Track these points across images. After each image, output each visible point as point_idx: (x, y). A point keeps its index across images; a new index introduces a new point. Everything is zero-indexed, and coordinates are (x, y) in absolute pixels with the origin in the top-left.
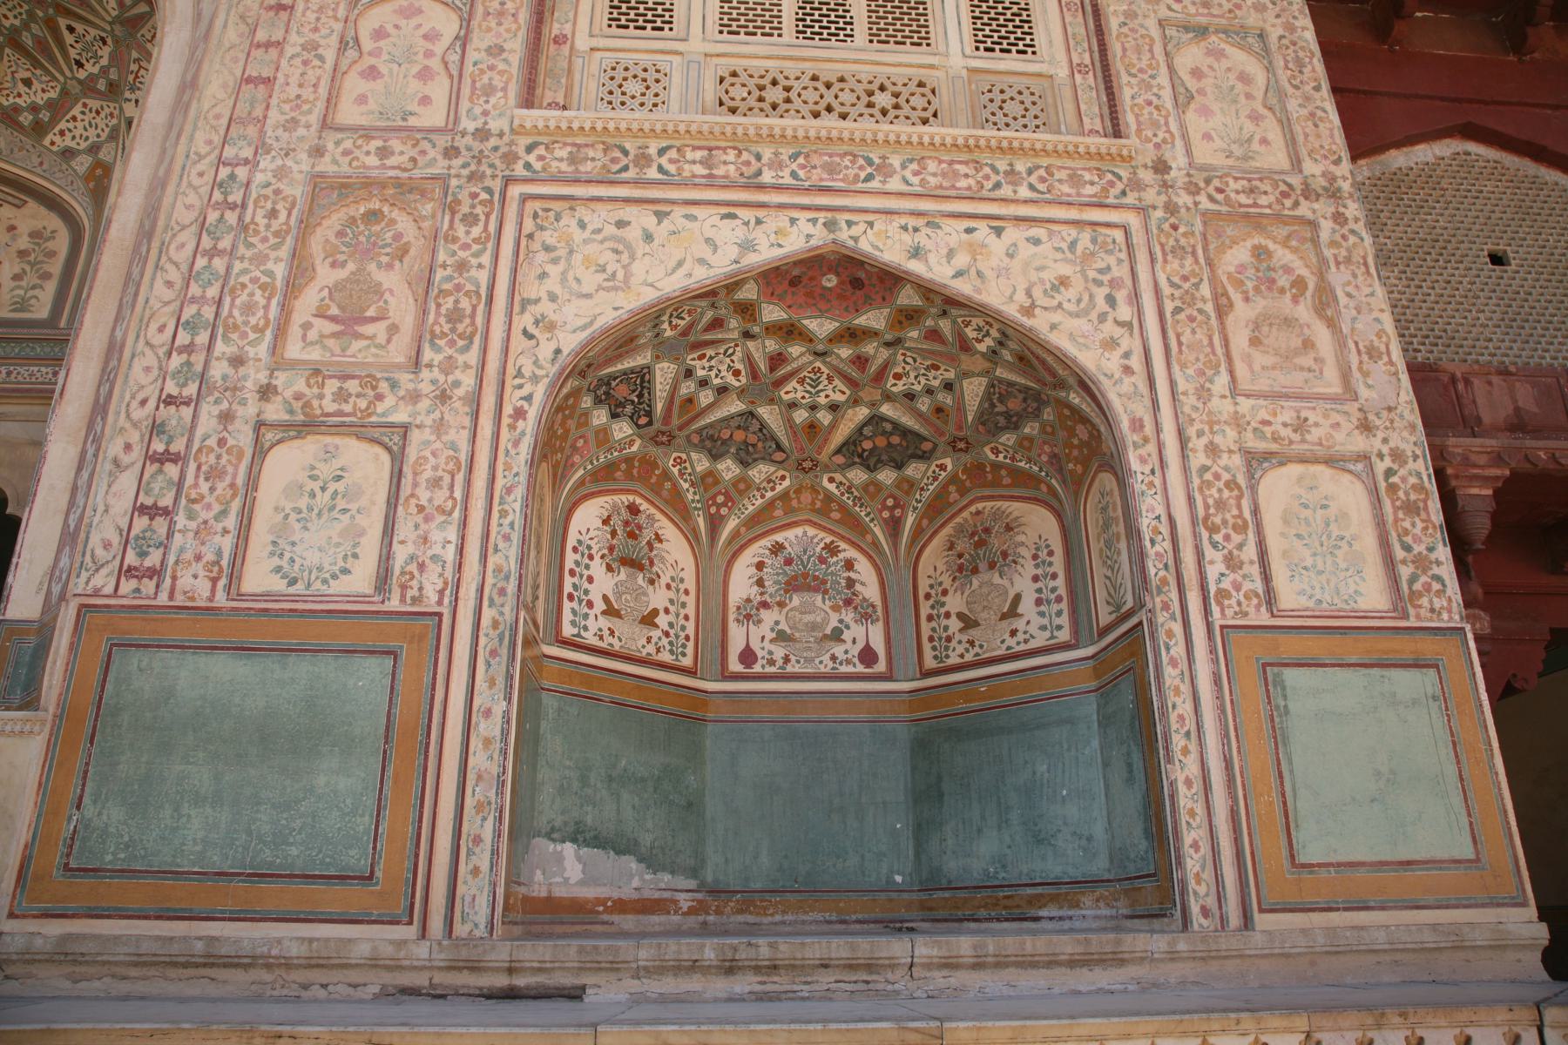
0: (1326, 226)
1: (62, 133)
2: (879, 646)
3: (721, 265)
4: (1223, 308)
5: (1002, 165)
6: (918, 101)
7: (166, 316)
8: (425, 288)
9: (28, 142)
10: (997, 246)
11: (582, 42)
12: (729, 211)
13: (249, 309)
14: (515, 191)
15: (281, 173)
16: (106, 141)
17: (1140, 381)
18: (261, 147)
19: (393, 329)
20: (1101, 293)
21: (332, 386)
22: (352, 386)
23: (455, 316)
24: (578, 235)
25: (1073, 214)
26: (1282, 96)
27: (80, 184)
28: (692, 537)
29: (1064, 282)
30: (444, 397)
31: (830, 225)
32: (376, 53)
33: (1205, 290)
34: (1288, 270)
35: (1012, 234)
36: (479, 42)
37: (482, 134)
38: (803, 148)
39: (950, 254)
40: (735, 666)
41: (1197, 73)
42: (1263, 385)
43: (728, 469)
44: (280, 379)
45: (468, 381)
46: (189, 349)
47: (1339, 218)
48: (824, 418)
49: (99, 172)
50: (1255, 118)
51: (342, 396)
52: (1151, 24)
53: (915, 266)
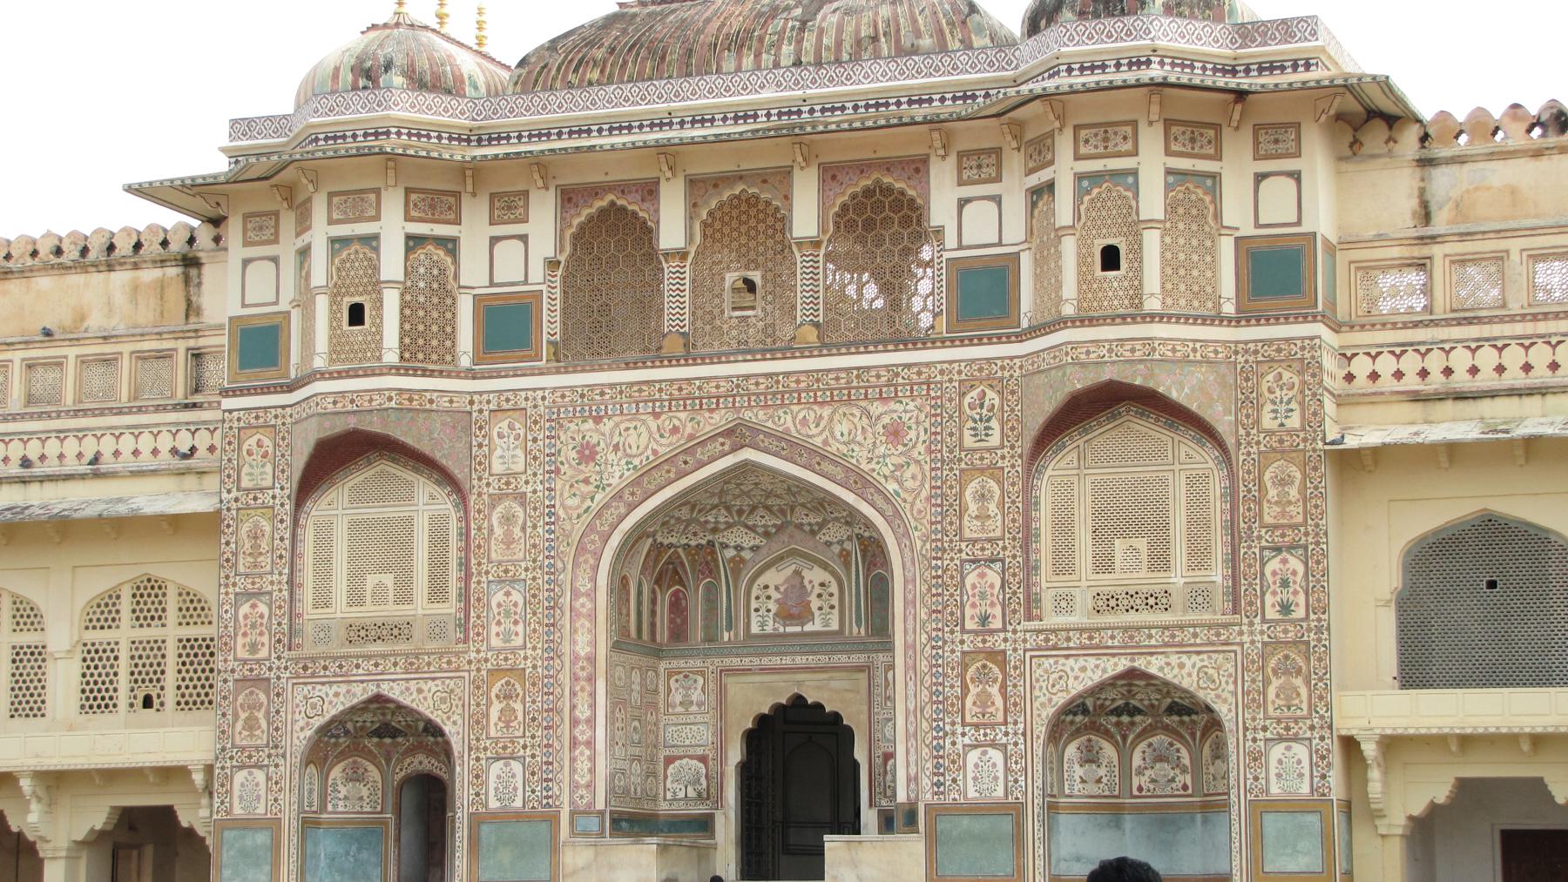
2: (1189, 782)
3: (1097, 677)
4: (1266, 682)
11: (1044, 585)
14: (1028, 654)
17: (1233, 714)
18: (945, 642)
23: (1015, 704)
28: (1116, 745)
30: (1015, 734)
31: (1133, 660)
40: (1135, 793)
41: (1274, 573)
43: (1125, 719)
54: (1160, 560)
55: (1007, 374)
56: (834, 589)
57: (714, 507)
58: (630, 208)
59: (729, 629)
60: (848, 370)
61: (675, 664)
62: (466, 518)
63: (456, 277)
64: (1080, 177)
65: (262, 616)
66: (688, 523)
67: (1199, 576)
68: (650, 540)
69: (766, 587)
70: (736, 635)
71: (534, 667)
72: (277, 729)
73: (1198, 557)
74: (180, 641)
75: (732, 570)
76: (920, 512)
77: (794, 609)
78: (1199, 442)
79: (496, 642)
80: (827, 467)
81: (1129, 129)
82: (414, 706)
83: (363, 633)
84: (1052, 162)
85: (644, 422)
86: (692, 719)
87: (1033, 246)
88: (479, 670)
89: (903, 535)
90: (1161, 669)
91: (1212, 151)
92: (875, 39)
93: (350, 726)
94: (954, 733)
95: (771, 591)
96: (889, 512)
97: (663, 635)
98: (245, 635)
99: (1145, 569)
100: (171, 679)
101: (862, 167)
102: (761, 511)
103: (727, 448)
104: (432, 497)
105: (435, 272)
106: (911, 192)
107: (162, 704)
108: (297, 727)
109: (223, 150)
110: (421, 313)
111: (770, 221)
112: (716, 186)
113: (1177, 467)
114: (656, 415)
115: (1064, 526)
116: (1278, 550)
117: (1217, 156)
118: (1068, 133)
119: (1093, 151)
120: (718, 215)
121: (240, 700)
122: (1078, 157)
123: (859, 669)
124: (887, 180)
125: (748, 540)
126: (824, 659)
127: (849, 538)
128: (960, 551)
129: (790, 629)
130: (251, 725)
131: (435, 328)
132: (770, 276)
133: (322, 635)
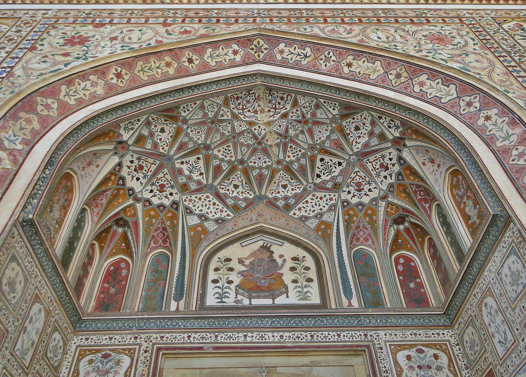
1: (300, 209)
16: (327, 211)
27: (312, 233)
49: (323, 226)
56: (310, 262)
59: (178, 298)
61: (94, 339)
66: (165, 161)
68: (116, 160)
70: (188, 304)
75: (192, 239)
77: (263, 277)
80: (361, 66)
85: (151, 28)
95: (234, 264)
102: (238, 177)
103: (238, 58)
114: (165, 24)
125: (214, 210)
127: (332, 208)
129: (256, 302)
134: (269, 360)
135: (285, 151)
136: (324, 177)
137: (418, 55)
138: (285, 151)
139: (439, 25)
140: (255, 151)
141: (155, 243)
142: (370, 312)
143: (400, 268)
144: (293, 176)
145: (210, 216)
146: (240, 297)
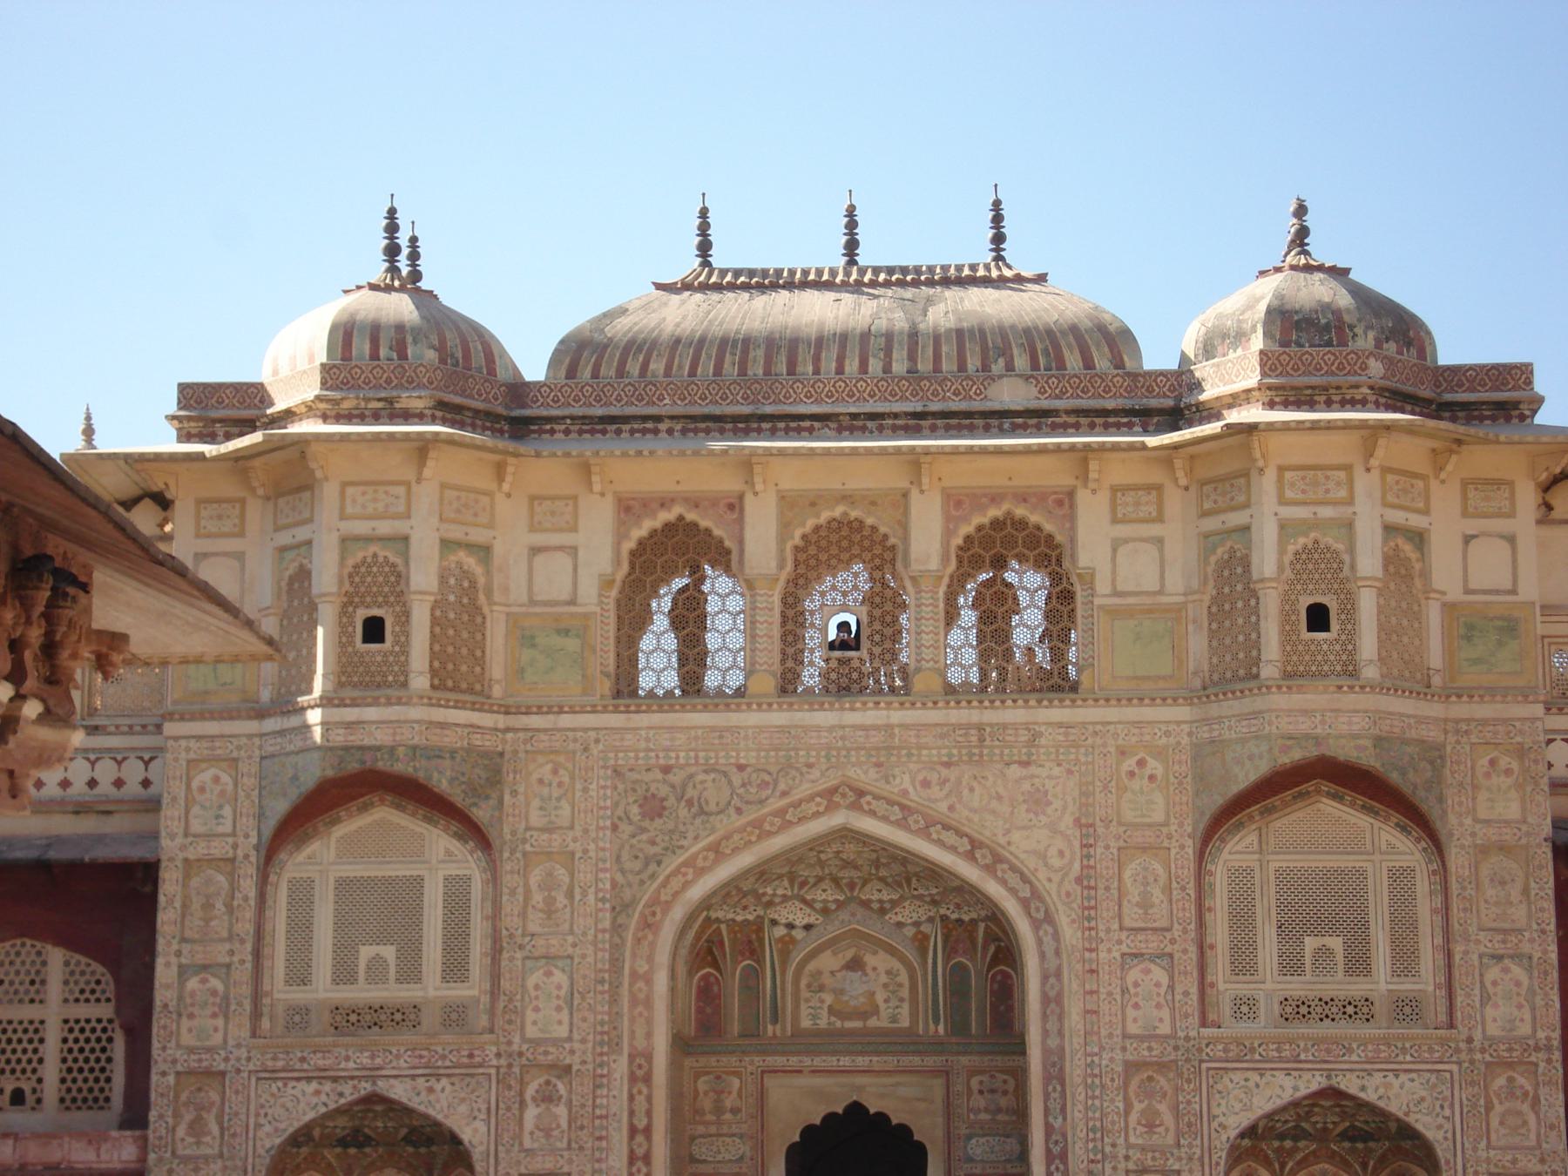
0: (1542, 1065)
3: (1288, 1097)
4: (1489, 1108)
5: (1400, 1045)
6: (1365, 1010)
7: (1081, 1125)
8: (1175, 1109)
9: (875, 916)
10: (1396, 1083)
11: (1221, 986)
12: (1288, 1072)
13: (1113, 1123)
14: (1204, 1066)
15: (1112, 1060)
19: (1167, 1130)
20: (1438, 1104)
21: (1150, 1155)
22: (1157, 1155)
23: (1189, 1125)
24: (1231, 1086)
25: (1429, 1067)
26: (1534, 994)
29: (1423, 1099)
30: (1190, 1159)
32: (1137, 995)
33: (1482, 1102)
34: (1522, 1087)
35: (1403, 1077)
36: (1179, 989)
37: (1187, 1039)
38: (1317, 1042)
39: (1377, 1089)
41: (1495, 983)
42: (1502, 1143)
43: (1288, 1144)
44: (1131, 1153)
45: (1198, 1151)
46: (1094, 1140)
47: (1549, 1061)
48: (1331, 1126)
50: (1520, 1007)
51: (1154, 1159)
52: (1475, 957)
53: (1362, 1095)
54: (1359, 963)
55: (1172, 740)
56: (904, 977)
57: (780, 877)
58: (704, 523)
59: (775, 1020)
60: (980, 728)
61: (703, 1060)
62: (494, 878)
63: (489, 592)
64: (1283, 526)
65: (214, 993)
67: (1406, 986)
69: (820, 973)
71: (584, 1062)
72: (234, 1135)
73: (1405, 960)
74: (66, 1021)
76: (1068, 894)
78: (1403, 829)
79: (531, 1031)
81: (1342, 475)
82: (422, 1108)
83: (353, 1018)
84: (1246, 505)
85: (725, 774)
86: (725, 1129)
87: (1207, 598)
88: (510, 1066)
89: (1044, 921)
90: (1363, 1088)
91: (1421, 505)
92: (1005, 351)
93: (316, 1133)
94: (1115, 1157)
95: (827, 980)
96: (1026, 892)
97: (691, 1030)
98: (191, 1016)
99: (1341, 974)
100: (51, 1072)
101: (995, 499)
104: (448, 853)
105: (466, 584)
106: (1048, 527)
107: (39, 1101)
108: (260, 1134)
109: (172, 418)
110: (451, 632)
111: (878, 550)
112: (813, 504)
113: (1377, 857)
115: (1242, 920)
116: (1499, 958)
117: (1426, 512)
118: (1270, 476)
119: (1300, 496)
120: (814, 538)
121: (184, 1097)
122: (1283, 501)
123: (934, 1073)
124: (1020, 512)
125: (800, 916)
126: (891, 1061)
127: (931, 920)
128: (1120, 942)
129: (849, 1024)
130: (197, 1128)
131: (464, 651)
132: (877, 612)
133: (297, 1018)
134: (860, 1080)
135: (877, 868)
136: (921, 891)
137: (1002, 841)
138: (877, 868)
139: (1048, 764)
140: (843, 868)
141: (742, 954)
142: (954, 1040)
143: (996, 986)
144: (887, 884)
145: (797, 923)
146: (833, 1019)
